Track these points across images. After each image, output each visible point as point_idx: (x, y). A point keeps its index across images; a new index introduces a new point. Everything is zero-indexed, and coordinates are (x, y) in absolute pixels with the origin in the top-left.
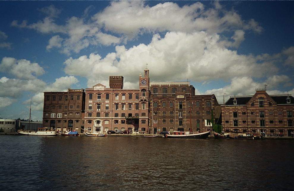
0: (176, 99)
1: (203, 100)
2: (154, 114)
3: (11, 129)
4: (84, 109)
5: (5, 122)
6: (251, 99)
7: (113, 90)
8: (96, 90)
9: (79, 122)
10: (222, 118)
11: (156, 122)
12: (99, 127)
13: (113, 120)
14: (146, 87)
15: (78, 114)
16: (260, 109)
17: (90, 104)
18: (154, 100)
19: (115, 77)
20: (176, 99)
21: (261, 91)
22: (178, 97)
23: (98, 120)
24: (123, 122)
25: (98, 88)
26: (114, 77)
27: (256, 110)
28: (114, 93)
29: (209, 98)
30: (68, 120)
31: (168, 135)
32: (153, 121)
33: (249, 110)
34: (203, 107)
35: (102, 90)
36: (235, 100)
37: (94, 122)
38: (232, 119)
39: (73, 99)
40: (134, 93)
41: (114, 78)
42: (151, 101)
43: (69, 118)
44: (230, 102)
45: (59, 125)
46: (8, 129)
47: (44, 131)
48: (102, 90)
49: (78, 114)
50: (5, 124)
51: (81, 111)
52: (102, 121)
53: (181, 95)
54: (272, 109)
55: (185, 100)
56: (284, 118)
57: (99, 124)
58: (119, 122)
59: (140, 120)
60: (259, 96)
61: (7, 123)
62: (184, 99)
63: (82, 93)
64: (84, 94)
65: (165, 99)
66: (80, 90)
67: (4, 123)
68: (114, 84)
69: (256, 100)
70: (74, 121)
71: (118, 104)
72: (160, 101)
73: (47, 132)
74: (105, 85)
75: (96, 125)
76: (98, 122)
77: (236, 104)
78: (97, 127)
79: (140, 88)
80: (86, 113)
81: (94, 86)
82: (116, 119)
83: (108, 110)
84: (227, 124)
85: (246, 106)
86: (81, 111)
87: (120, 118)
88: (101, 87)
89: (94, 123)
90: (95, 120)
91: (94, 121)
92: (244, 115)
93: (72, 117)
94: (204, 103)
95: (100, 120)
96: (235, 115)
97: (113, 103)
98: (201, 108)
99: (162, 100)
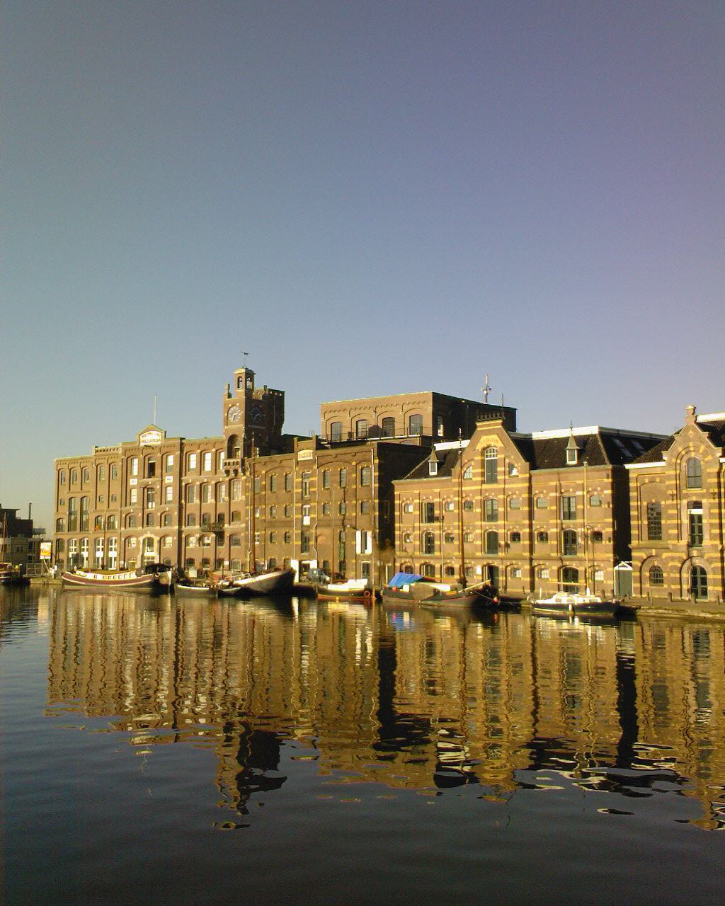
23: (149, 535)
52: (156, 539)
54: (518, 489)
62: (312, 462)
65: (276, 465)
72: (264, 472)
77: (435, 473)
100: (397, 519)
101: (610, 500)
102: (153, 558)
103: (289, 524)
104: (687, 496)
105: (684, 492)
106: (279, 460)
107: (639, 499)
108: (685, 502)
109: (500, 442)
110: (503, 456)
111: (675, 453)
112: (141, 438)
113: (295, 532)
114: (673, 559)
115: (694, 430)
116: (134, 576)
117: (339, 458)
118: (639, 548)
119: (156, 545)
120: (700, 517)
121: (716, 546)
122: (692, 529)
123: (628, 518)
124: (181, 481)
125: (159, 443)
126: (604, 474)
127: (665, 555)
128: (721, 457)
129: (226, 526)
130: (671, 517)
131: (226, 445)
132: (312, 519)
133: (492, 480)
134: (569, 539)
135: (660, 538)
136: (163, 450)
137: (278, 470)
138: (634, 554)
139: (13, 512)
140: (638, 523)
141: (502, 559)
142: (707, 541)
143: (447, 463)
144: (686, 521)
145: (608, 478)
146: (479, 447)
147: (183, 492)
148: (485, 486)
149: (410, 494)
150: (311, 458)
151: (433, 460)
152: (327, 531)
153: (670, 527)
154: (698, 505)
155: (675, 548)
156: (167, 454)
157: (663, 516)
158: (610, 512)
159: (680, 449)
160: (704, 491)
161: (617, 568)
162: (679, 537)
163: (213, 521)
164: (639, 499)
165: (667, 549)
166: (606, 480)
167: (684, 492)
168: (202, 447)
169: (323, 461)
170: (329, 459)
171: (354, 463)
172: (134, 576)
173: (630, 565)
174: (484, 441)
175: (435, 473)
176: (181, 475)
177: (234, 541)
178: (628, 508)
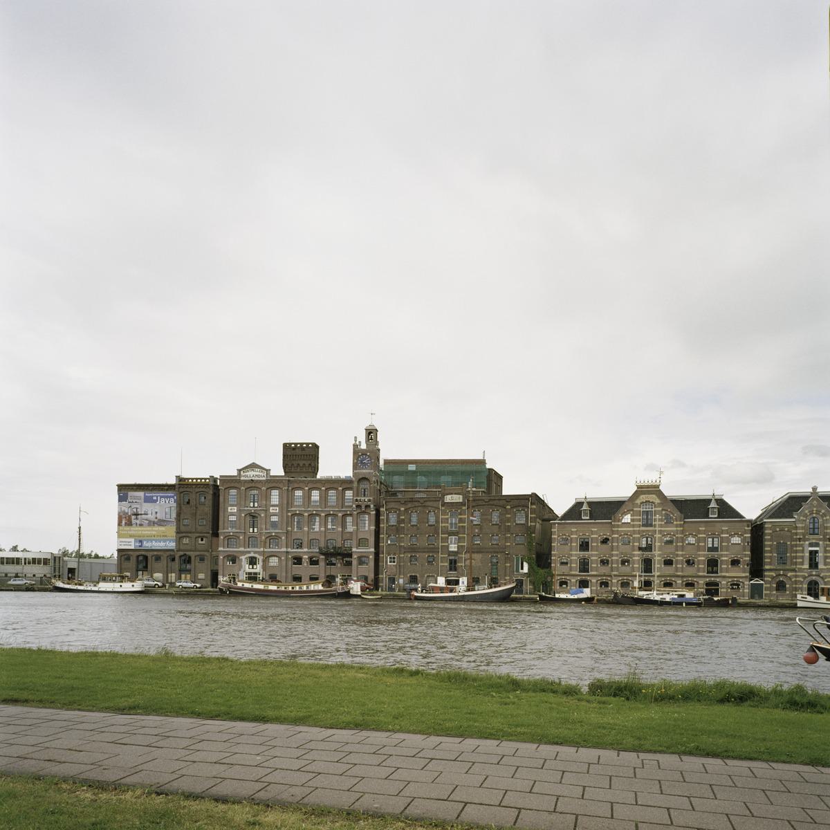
0: (443, 505)
1: (509, 507)
2: (389, 542)
3: (41, 578)
4: (218, 530)
5: (25, 559)
6: (624, 506)
7: (289, 481)
8: (245, 481)
9: (206, 561)
11: (394, 562)
12: (256, 574)
13: (290, 557)
14: (370, 473)
15: (202, 540)
16: (644, 531)
17: (232, 514)
18: (388, 507)
19: (296, 444)
20: (443, 505)
21: (648, 487)
22: (448, 499)
23: (252, 555)
24: (313, 562)
25: (251, 474)
26: (293, 445)
27: (634, 532)
28: (290, 488)
29: (523, 502)
30: (178, 555)
31: (416, 594)
32: (387, 558)
33: (617, 532)
34: (507, 524)
35: (261, 479)
36: (585, 507)
37: (244, 560)
38: (576, 555)
39: (188, 503)
40: (341, 488)
41: (294, 449)
42: (381, 509)
43: (182, 551)
44: (575, 512)
45: (157, 565)
46: (34, 575)
47: (114, 581)
48: (261, 481)
49: (202, 540)
50: (25, 564)
51: (209, 533)
52: (260, 558)
53: (455, 494)
54: (672, 531)
55: (464, 508)
56: (699, 553)
57: (255, 567)
58: (303, 560)
59: (355, 557)
60: (643, 498)
61: (29, 563)
62: (462, 504)
63: (211, 487)
64: (216, 487)
65: (417, 504)
66: (205, 479)
67: (23, 563)
68: (295, 463)
69: (635, 509)
70: (193, 558)
71: (300, 515)
72: (402, 509)
73: (121, 584)
74: (267, 468)
75: (247, 568)
76: (253, 561)
77: (588, 518)
78: (250, 573)
79: (354, 474)
80: (222, 537)
81: (239, 471)
82: (295, 554)
83: (277, 531)
84: (564, 567)
85: (611, 523)
86: (211, 532)
87: (306, 550)
88: (261, 474)
89: (243, 563)
90: (246, 556)
91: (243, 558)
92: (604, 546)
93: (189, 548)
94: (509, 516)
95: (256, 555)
96: (584, 546)
97: (290, 514)
98: (502, 527)
99: (410, 505)
101: (749, 541)
103: (435, 550)
104: (808, 540)
105: (807, 537)
108: (807, 543)
110: (660, 509)
115: (817, 501)
117: (491, 502)
118: (770, 570)
122: (811, 559)
125: (264, 479)
126: (745, 524)
131: (355, 485)
134: (713, 564)
137: (420, 508)
140: (770, 556)
144: (807, 554)
150: (461, 501)
154: (817, 545)
158: (749, 548)
160: (821, 537)
162: (802, 563)
166: (746, 528)
167: (807, 537)
170: (480, 503)
172: (320, 587)
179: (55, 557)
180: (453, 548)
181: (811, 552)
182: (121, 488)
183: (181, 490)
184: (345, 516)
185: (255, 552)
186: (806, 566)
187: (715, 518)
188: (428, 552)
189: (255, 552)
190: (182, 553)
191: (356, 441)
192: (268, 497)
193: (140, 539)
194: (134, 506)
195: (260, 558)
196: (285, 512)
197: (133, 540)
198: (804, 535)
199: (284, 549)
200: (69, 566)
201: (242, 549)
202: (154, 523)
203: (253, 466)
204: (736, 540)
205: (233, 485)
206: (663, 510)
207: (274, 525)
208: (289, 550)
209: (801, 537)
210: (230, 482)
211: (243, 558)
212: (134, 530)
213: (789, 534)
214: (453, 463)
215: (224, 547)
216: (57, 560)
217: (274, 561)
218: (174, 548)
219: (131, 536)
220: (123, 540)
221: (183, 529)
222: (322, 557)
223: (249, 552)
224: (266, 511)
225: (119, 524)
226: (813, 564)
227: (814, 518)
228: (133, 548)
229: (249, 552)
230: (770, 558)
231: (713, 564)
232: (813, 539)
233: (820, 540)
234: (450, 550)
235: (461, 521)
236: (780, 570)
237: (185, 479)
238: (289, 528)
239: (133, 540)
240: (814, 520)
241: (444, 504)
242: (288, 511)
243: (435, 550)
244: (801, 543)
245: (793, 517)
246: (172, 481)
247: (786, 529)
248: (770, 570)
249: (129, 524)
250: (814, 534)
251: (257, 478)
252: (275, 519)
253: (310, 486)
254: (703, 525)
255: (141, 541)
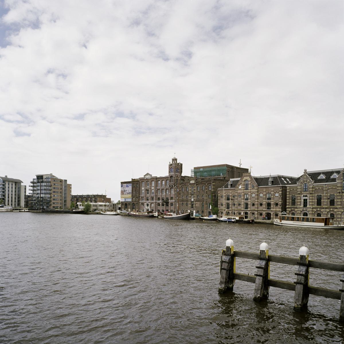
10: (219, 201)
23: (147, 203)
25: (147, 177)
48: (149, 179)
52: (149, 204)
53: (193, 180)
54: (254, 191)
62: (194, 184)
66: (138, 179)
72: (180, 186)
78: (147, 209)
81: (144, 176)
87: (161, 201)
91: (145, 204)
95: (148, 203)
100: (219, 199)
102: (148, 209)
103: (187, 201)
104: (303, 194)
105: (302, 193)
106: (185, 183)
107: (289, 194)
108: (302, 195)
109: (249, 179)
110: (250, 182)
111: (300, 182)
112: (145, 177)
113: (189, 203)
114: (298, 211)
116: (147, 214)
117: (202, 183)
118: (288, 208)
119: (149, 206)
120: (306, 199)
121: (311, 207)
122: (304, 203)
123: (286, 199)
124: (156, 188)
126: (280, 188)
127: (296, 210)
128: (314, 183)
129: (169, 201)
130: (298, 199)
131: (169, 178)
132: (194, 199)
133: (247, 189)
134: (269, 205)
135: (295, 205)
136: (151, 180)
137: (184, 186)
138: (287, 209)
139: (105, 196)
140: (289, 201)
141: (249, 210)
142: (308, 206)
143: (234, 185)
144: (303, 201)
145: (281, 189)
146: (243, 180)
147: (157, 191)
148: (245, 191)
149: (223, 193)
151: (230, 183)
152: (199, 203)
153: (298, 202)
154: (306, 196)
155: (299, 208)
156: (152, 181)
157: (296, 199)
159: (302, 181)
160: (308, 192)
161: (282, 213)
162: (300, 205)
163: (165, 199)
164: (289, 194)
165: (297, 208)
166: (280, 189)
167: (302, 193)
168: (162, 179)
169: (197, 183)
170: (199, 183)
171: (206, 184)
173: (286, 212)
174: (245, 178)
175: (230, 187)
176: (156, 187)
177: (172, 204)
178: (286, 197)
179: (113, 204)
180: (192, 200)
181: (304, 199)
182: (122, 183)
183: (133, 183)
184: (166, 189)
185: (148, 202)
186: (302, 206)
187: (271, 185)
188: (186, 201)
189: (148, 202)
190: (133, 203)
191: (170, 163)
192: (151, 184)
193: (125, 198)
194: (124, 188)
195: (149, 204)
196: (155, 188)
197: (124, 199)
198: (301, 191)
199: (155, 201)
200: (119, 207)
201: (145, 201)
202: (128, 193)
203: (148, 174)
204: (277, 195)
205: (143, 181)
206: (251, 183)
207: (153, 193)
208: (157, 201)
209: (300, 193)
210: (142, 180)
211: (145, 204)
212: (124, 196)
213: (296, 191)
214: (215, 167)
215: (141, 201)
216: (114, 205)
217: (153, 205)
218: (131, 201)
219: (123, 198)
220: (122, 199)
221: (133, 195)
222: (165, 203)
223: (147, 202)
224: (151, 188)
225: (121, 194)
226: (305, 205)
227: (306, 184)
228: (124, 201)
229: (147, 202)
230: (289, 202)
231: (269, 205)
232: (305, 193)
233: (308, 194)
234: (192, 200)
235: (194, 190)
236: (292, 208)
237: (135, 179)
238: (157, 194)
239: (124, 199)
240: (306, 185)
241: (190, 184)
242: (157, 188)
243: (187, 201)
244: (300, 195)
245: (335, 182)
246: (130, 180)
247: (295, 189)
248: (288, 208)
249: (123, 194)
250: (306, 191)
251: (148, 178)
252: (153, 191)
253: (162, 179)
254: (265, 188)
255: (125, 199)
